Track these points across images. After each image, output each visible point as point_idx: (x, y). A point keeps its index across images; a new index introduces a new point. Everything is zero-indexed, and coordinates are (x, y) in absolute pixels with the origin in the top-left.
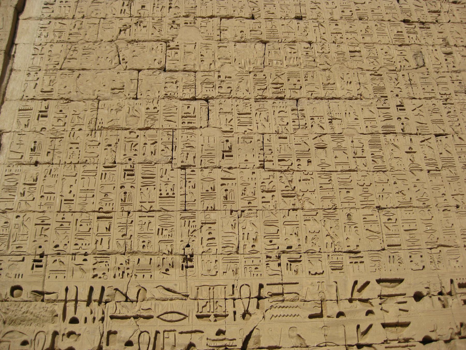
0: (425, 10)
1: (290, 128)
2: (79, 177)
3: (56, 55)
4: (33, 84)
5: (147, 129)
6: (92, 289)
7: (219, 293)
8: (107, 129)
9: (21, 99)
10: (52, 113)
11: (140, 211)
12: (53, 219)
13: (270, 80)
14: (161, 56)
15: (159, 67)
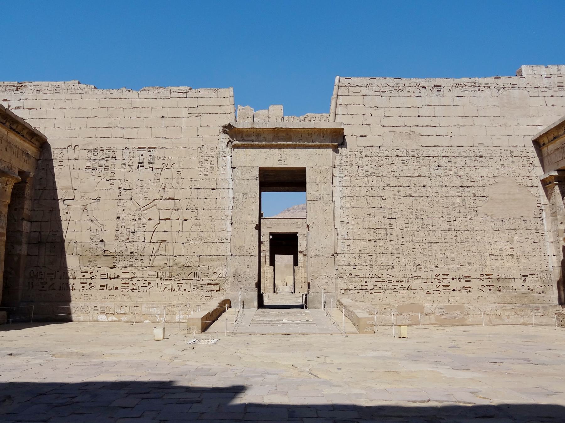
0: (470, 181)
1: (420, 228)
7: (401, 276)
13: (414, 212)
14: (380, 203)
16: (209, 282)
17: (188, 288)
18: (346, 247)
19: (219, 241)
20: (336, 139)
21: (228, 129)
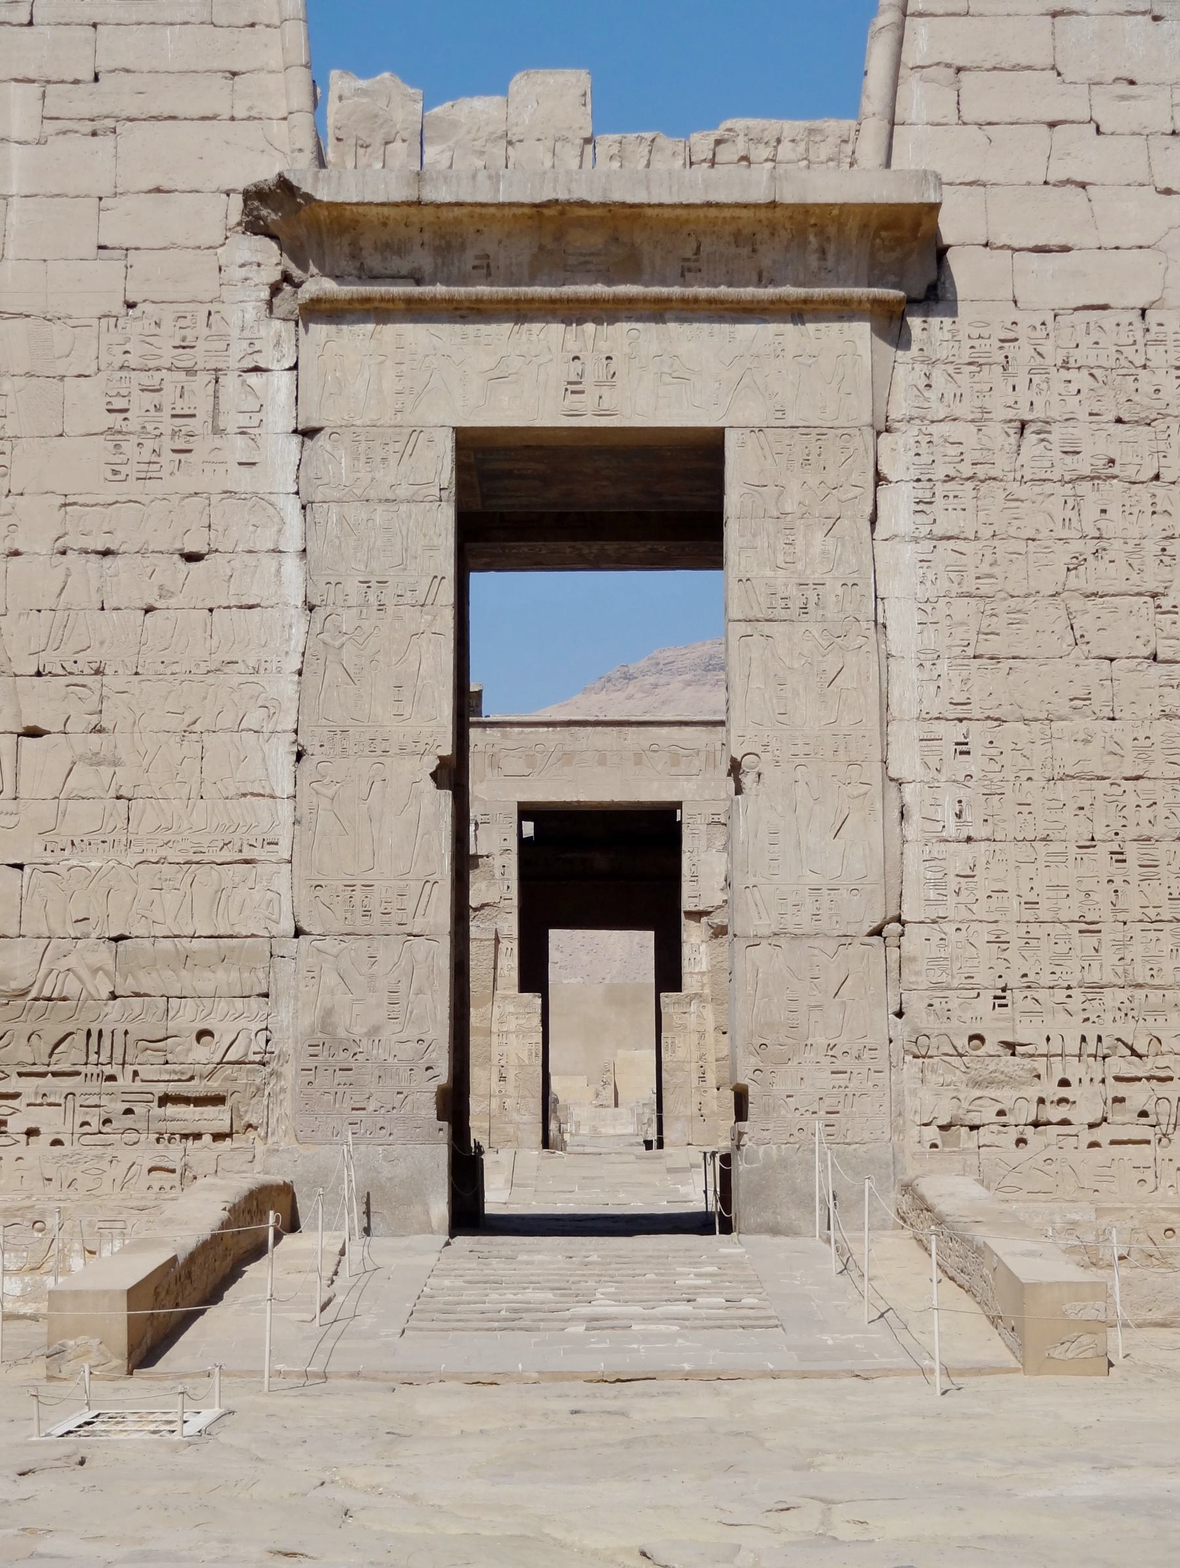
2: (1041, 864)
3: (962, 624)
4: (933, 689)
5: (1137, 778)
6: (1083, 1039)
8: (1073, 777)
9: (918, 718)
10: (976, 744)
11: (1141, 921)
12: (1014, 934)
14: (1147, 631)
15: (1146, 655)
16: (172, 1089)
17: (49, 1121)
18: (953, 883)
19: (226, 855)
20: (898, 265)
21: (276, 209)
